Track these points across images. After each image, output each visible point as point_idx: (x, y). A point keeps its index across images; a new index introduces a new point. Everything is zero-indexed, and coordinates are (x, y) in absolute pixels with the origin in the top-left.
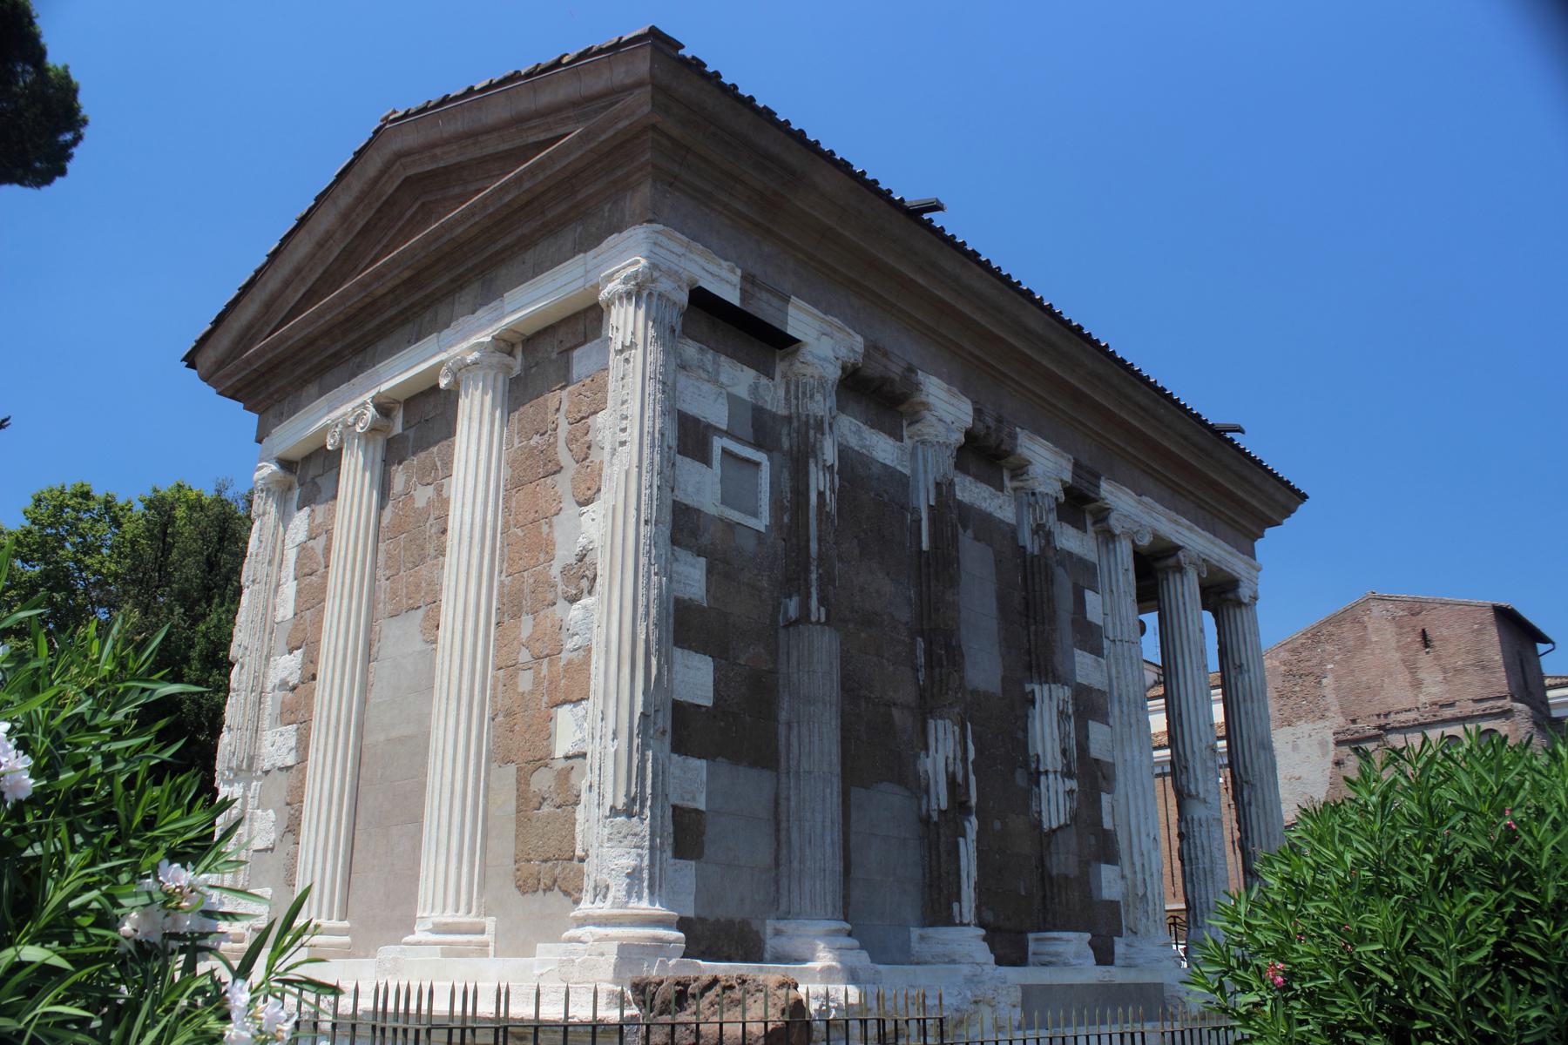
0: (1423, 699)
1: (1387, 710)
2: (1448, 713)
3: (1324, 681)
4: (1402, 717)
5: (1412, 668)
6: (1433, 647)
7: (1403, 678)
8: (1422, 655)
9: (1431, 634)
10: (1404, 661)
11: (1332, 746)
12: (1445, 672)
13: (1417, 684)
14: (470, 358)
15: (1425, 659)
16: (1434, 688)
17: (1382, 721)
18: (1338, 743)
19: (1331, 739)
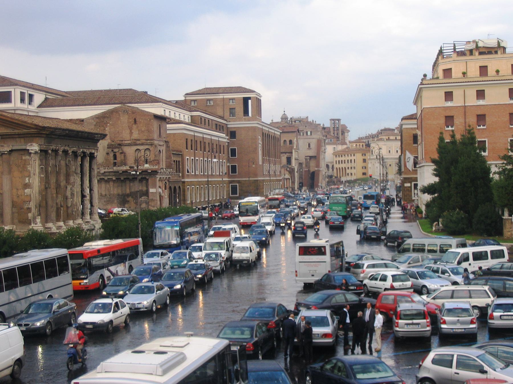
0: (132, 138)
1: (122, 139)
2: (138, 142)
3: (106, 129)
4: (126, 142)
5: (131, 129)
6: (137, 124)
7: (128, 131)
8: (134, 125)
9: (137, 120)
10: (129, 126)
11: (106, 148)
12: (139, 131)
13: (131, 133)
14: (6, 152)
15: (135, 126)
16: (135, 135)
17: (121, 142)
18: (108, 148)
19: (106, 146)
